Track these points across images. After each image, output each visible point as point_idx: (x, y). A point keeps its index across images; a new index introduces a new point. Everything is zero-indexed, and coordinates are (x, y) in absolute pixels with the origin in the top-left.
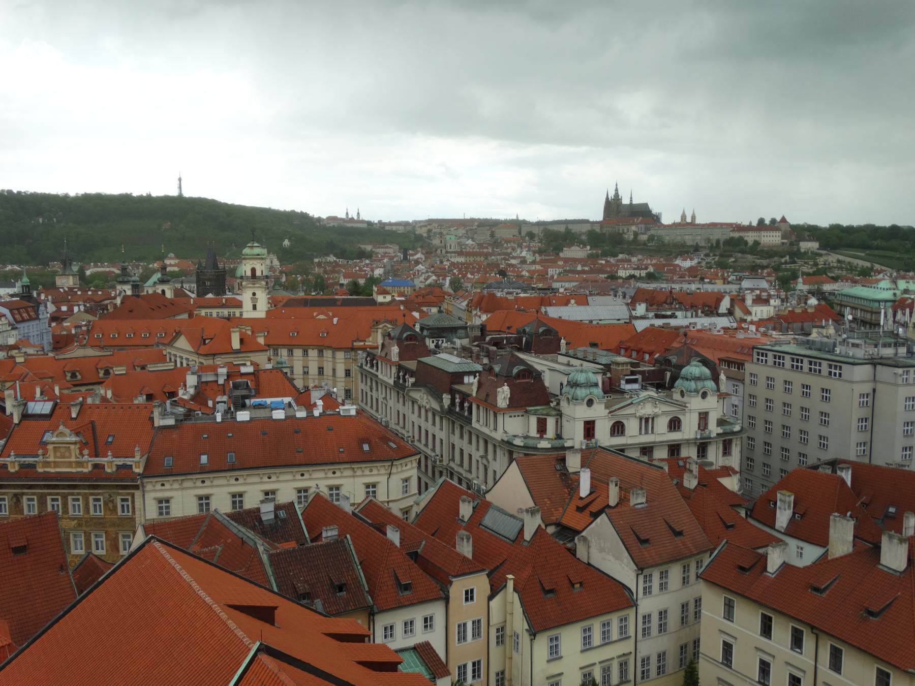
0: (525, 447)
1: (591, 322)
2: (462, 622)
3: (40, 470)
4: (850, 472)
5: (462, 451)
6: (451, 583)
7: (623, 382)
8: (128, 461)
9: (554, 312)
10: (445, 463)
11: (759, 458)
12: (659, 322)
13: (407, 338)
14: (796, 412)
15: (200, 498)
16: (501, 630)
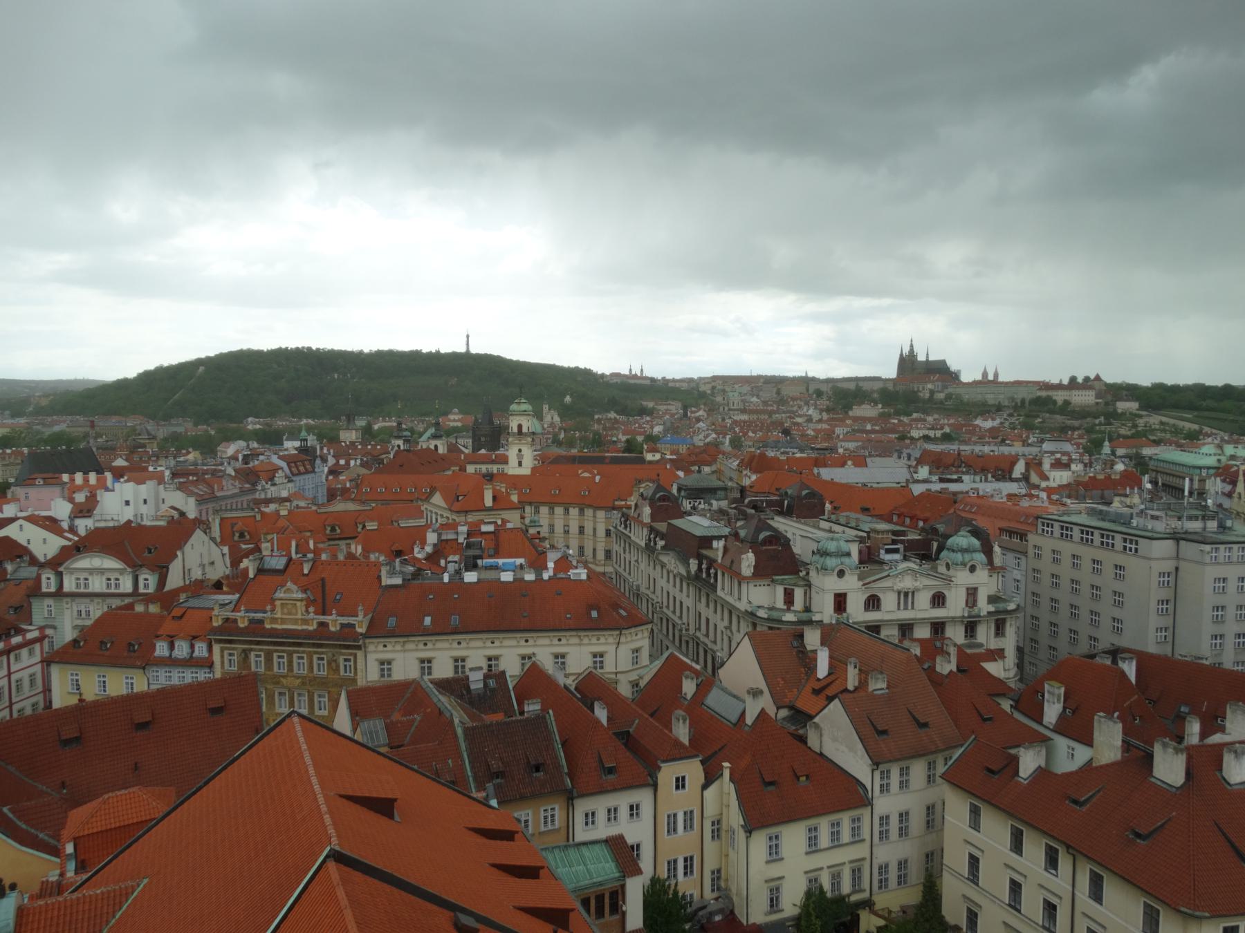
0: (768, 619)
1: (865, 485)
2: (671, 812)
3: (268, 626)
4: (1134, 663)
5: (708, 620)
6: (659, 768)
7: (882, 552)
8: (351, 620)
9: (826, 474)
10: (691, 632)
11: (1044, 640)
12: (937, 487)
13: (660, 499)
14: (1085, 589)
15: (422, 661)
16: (717, 823)
